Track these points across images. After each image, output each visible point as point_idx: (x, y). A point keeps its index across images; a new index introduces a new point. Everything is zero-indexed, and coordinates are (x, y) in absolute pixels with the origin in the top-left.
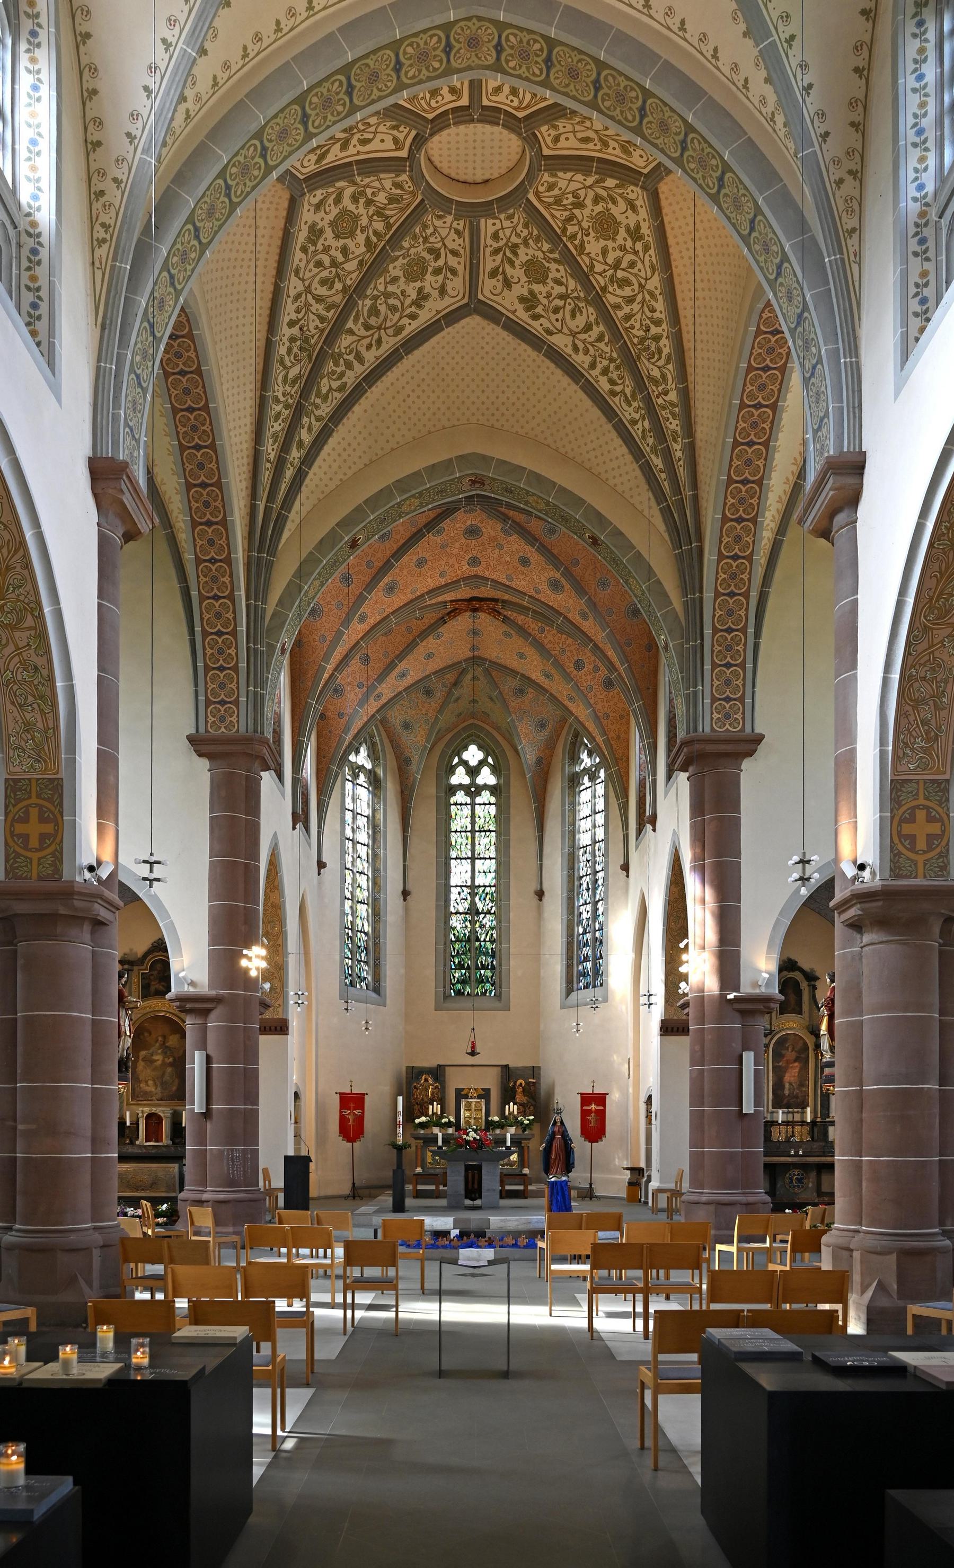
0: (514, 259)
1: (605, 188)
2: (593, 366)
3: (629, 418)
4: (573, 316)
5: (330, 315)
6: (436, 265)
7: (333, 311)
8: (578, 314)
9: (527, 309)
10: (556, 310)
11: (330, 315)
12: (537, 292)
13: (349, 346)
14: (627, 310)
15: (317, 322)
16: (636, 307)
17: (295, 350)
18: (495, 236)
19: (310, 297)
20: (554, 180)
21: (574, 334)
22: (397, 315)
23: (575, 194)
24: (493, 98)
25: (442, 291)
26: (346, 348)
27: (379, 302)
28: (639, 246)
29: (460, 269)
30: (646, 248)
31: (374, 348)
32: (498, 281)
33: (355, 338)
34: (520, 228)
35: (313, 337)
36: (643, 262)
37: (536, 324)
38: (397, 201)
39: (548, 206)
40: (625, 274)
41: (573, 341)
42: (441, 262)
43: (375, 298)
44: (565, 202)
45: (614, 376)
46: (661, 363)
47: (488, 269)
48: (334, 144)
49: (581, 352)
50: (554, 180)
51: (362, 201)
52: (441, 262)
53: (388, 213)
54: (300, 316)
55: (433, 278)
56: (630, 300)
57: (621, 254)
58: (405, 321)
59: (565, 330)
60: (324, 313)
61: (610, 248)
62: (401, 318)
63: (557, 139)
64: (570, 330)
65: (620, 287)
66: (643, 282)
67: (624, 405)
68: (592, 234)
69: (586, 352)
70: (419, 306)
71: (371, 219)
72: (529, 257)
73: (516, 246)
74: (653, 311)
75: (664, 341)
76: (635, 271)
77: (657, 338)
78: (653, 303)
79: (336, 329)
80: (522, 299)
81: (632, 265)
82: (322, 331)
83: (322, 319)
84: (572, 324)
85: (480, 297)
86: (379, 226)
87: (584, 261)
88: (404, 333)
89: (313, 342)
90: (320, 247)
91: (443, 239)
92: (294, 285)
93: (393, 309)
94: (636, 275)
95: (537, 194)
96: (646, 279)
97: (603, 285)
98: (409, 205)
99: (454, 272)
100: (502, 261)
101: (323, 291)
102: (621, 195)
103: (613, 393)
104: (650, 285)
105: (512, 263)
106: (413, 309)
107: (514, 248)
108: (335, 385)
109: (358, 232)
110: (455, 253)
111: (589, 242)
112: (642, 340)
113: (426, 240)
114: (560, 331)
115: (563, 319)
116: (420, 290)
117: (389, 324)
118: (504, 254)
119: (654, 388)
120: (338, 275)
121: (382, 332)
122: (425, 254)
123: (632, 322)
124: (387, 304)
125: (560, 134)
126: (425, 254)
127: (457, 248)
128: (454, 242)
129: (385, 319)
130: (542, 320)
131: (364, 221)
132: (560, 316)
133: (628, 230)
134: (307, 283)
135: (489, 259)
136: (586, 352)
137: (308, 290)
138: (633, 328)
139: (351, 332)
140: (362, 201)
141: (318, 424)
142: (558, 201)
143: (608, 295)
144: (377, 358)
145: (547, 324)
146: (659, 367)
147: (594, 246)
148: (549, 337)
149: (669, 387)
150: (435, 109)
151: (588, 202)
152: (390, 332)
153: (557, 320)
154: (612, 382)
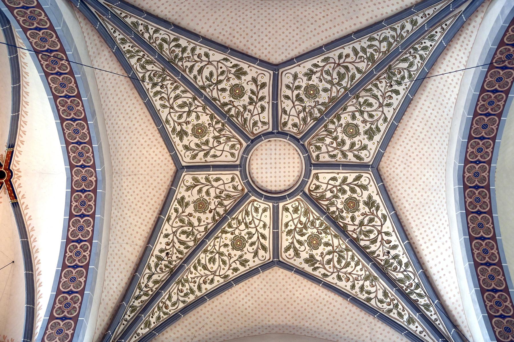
0: (251, 95)
1: (204, 150)
2: (193, 50)
3: (161, 32)
4: (211, 74)
5: (370, 86)
6: (298, 91)
7: (368, 88)
8: (208, 76)
9: (241, 69)
10: (222, 73)
11: (370, 86)
12: (236, 79)
13: (361, 61)
14: (178, 92)
15: (379, 85)
16: (173, 95)
17: (399, 76)
18: (263, 108)
19: (381, 101)
20: (232, 151)
21: (210, 63)
22: (326, 69)
23: (219, 143)
24: (267, 206)
25: (295, 77)
26: (363, 61)
27: (337, 81)
28: (178, 128)
29: (284, 88)
30: (174, 130)
31: (344, 54)
32: (260, 81)
33: (356, 65)
34: (249, 117)
35: (385, 78)
36: (174, 121)
37: (235, 62)
38: (319, 139)
39: (234, 137)
40: (183, 110)
41: (209, 59)
42: (296, 92)
43: (339, 84)
44: (225, 138)
45: (177, 50)
46: (147, 75)
47: (267, 88)
48: (350, 183)
49: (203, 54)
50: (232, 151)
51: (339, 140)
52: (296, 92)
53: (325, 133)
54: (390, 93)
55: (301, 84)
56: (177, 97)
57: (188, 120)
58: (321, 64)
59: (215, 63)
60: (374, 88)
61: (195, 120)
62: (324, 66)
63: (233, 179)
64: (212, 64)
65: (185, 102)
66: (172, 111)
67: (167, 37)
68: (207, 125)
69: (199, 56)
70: (311, 70)
71: (336, 130)
72: (242, 99)
73: (250, 104)
74: (161, 99)
75: (149, 86)
76: (177, 114)
77: (155, 85)
78: (162, 102)
79: (368, 77)
80: (245, 73)
81: (180, 117)
82: (377, 79)
83: (376, 86)
84: (211, 68)
85: (271, 72)
86: (331, 126)
87: (209, 111)
88: (323, 57)
89: (385, 75)
90: (368, 125)
91: (294, 106)
92: (389, 113)
93: (328, 73)
94: (177, 112)
95: (241, 144)
96: (170, 113)
97: (196, 101)
98: (313, 138)
99: (288, 87)
100: (258, 93)
101: (371, 100)
102: (194, 150)
103: (176, 40)
104: (167, 111)
105: (253, 92)
106: (315, 70)
107: (251, 101)
108: (376, 43)
109: (344, 125)
110: (287, 97)
111: (208, 120)
112: (164, 79)
113: (304, 109)
114: (218, 62)
115: (217, 69)
116: (310, 79)
117: (332, 65)
118: (257, 97)
119: (148, 58)
120: (361, 106)
121: (337, 62)
122: (306, 99)
123: (173, 87)
124: (332, 77)
125: (231, 182)
126: (306, 99)
127: (286, 101)
128: (287, 105)
129: (334, 69)
130: (231, 65)
131: (339, 129)
132: (220, 70)
133: (186, 134)
134: (381, 109)
135: (266, 94)
136: (199, 56)
137: (381, 105)
138: (172, 84)
139: (359, 70)
140: (339, 140)
141: (396, 27)
142: (228, 139)
143: (191, 96)
144: (343, 48)
145: (228, 64)
146: (148, 71)
147: (205, 119)
148: (225, 57)
149: (138, 64)
150: (296, 200)
151: (211, 140)
152: (331, 60)
153: (221, 68)
154: (178, 46)
